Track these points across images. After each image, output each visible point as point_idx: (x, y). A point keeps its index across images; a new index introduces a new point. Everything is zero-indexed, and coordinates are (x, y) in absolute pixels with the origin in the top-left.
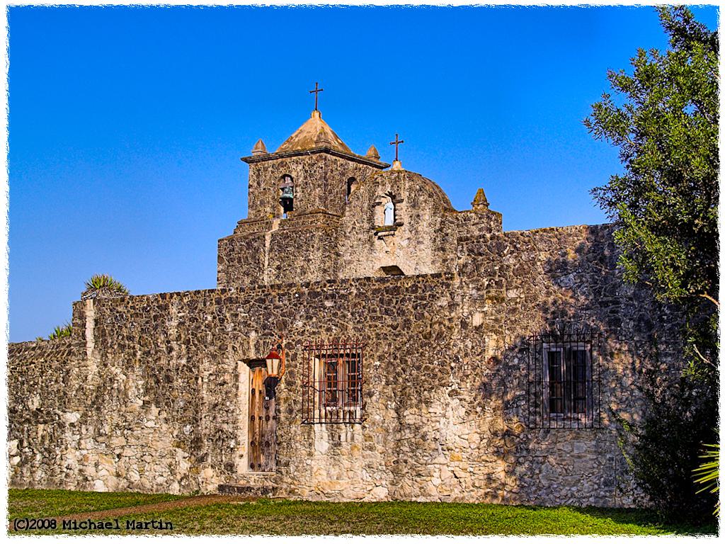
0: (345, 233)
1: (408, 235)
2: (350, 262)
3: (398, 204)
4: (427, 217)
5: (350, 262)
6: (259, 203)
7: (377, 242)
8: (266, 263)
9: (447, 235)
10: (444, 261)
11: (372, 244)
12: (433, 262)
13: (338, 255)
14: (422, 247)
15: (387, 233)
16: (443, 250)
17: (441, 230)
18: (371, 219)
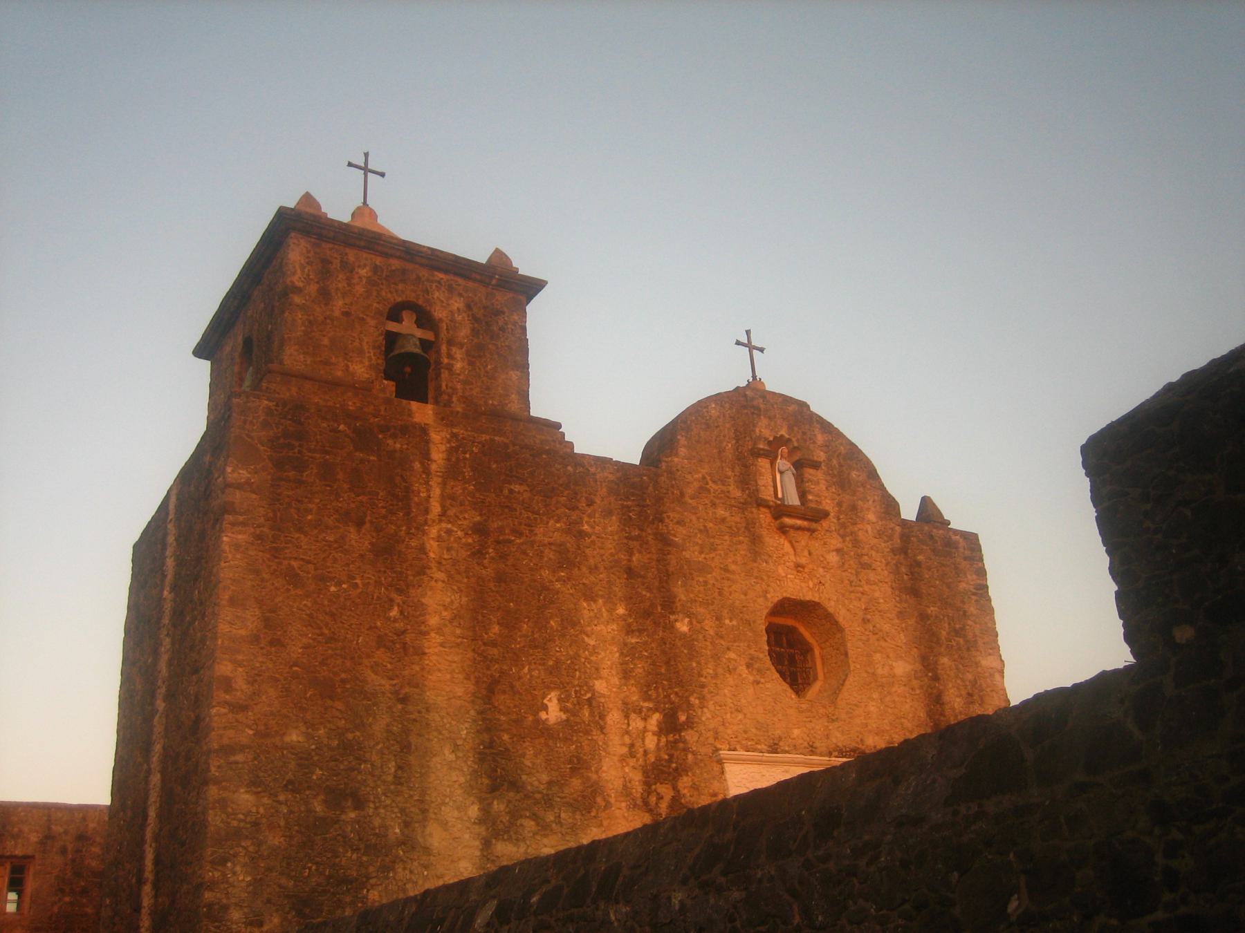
0: (682, 495)
1: (836, 542)
2: (704, 569)
3: (812, 471)
4: (871, 517)
5: (704, 569)
6: (326, 341)
7: (773, 541)
8: (436, 508)
9: (919, 564)
10: (923, 617)
11: (755, 540)
12: (901, 615)
13: (664, 541)
14: (872, 576)
15: (805, 523)
16: (915, 592)
17: (904, 550)
18: (747, 480)
